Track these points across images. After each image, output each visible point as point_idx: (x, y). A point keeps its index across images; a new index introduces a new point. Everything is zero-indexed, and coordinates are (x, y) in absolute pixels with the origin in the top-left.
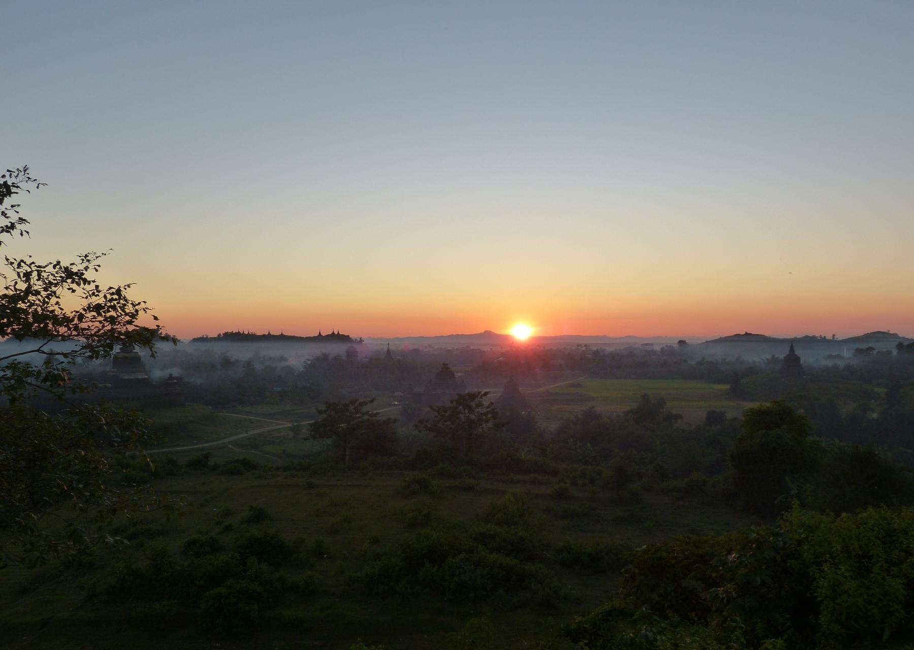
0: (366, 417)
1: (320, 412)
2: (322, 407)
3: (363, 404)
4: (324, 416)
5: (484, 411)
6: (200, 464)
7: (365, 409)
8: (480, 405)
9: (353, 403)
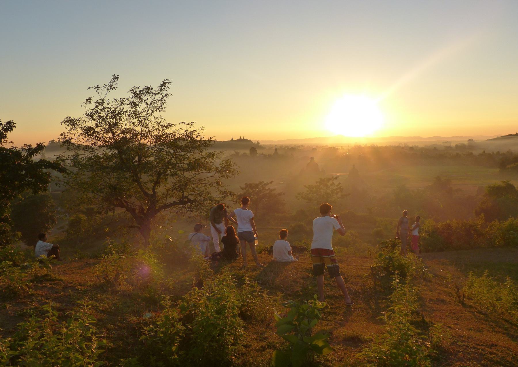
1: (242, 188)
2: (244, 186)
4: (245, 191)
7: (267, 187)
8: (333, 184)
9: (260, 183)
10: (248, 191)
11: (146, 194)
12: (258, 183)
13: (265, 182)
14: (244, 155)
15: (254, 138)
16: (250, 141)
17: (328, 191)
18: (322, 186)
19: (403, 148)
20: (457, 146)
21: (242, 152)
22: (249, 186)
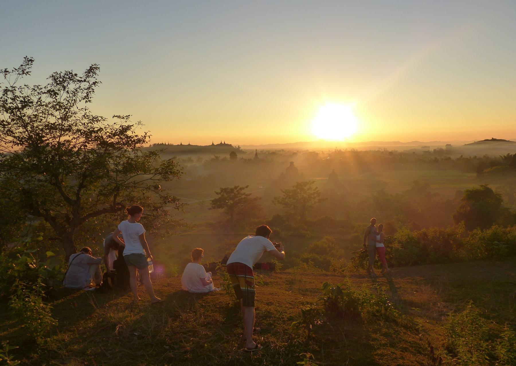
0: (243, 196)
1: (217, 193)
2: (219, 191)
4: (220, 196)
5: (312, 192)
7: (243, 192)
9: (236, 188)
10: (223, 195)
11: (67, 199)
12: (233, 187)
14: (224, 160)
15: (234, 144)
17: (305, 196)
18: (299, 190)
19: (382, 152)
20: (435, 150)
21: (222, 156)
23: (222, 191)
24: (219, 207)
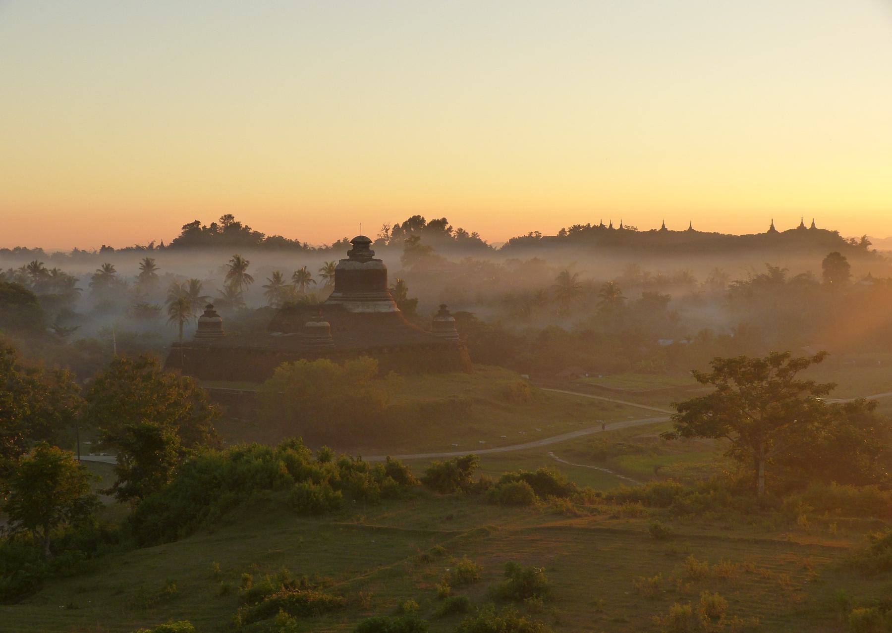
1: (702, 379)
2: (709, 371)
3: (797, 365)
4: (710, 389)
6: (446, 480)
7: (801, 377)
9: (776, 360)
10: (723, 388)
13: (795, 356)
16: (836, 233)
22: (726, 368)
23: (719, 370)
24: (705, 431)
